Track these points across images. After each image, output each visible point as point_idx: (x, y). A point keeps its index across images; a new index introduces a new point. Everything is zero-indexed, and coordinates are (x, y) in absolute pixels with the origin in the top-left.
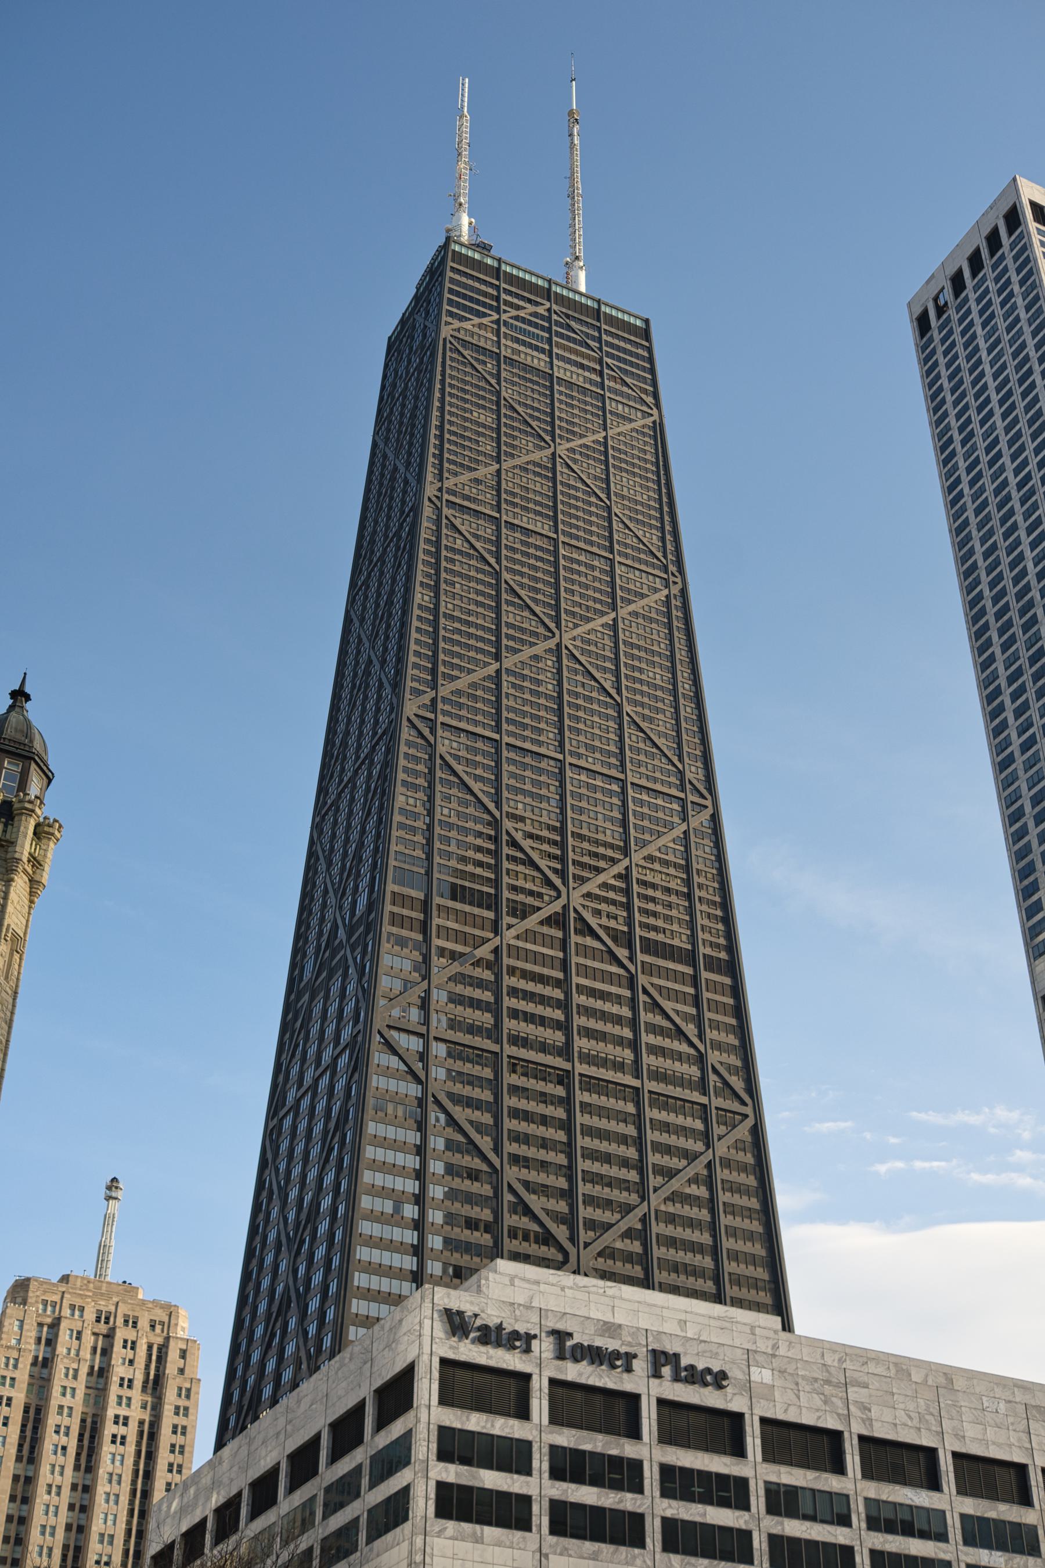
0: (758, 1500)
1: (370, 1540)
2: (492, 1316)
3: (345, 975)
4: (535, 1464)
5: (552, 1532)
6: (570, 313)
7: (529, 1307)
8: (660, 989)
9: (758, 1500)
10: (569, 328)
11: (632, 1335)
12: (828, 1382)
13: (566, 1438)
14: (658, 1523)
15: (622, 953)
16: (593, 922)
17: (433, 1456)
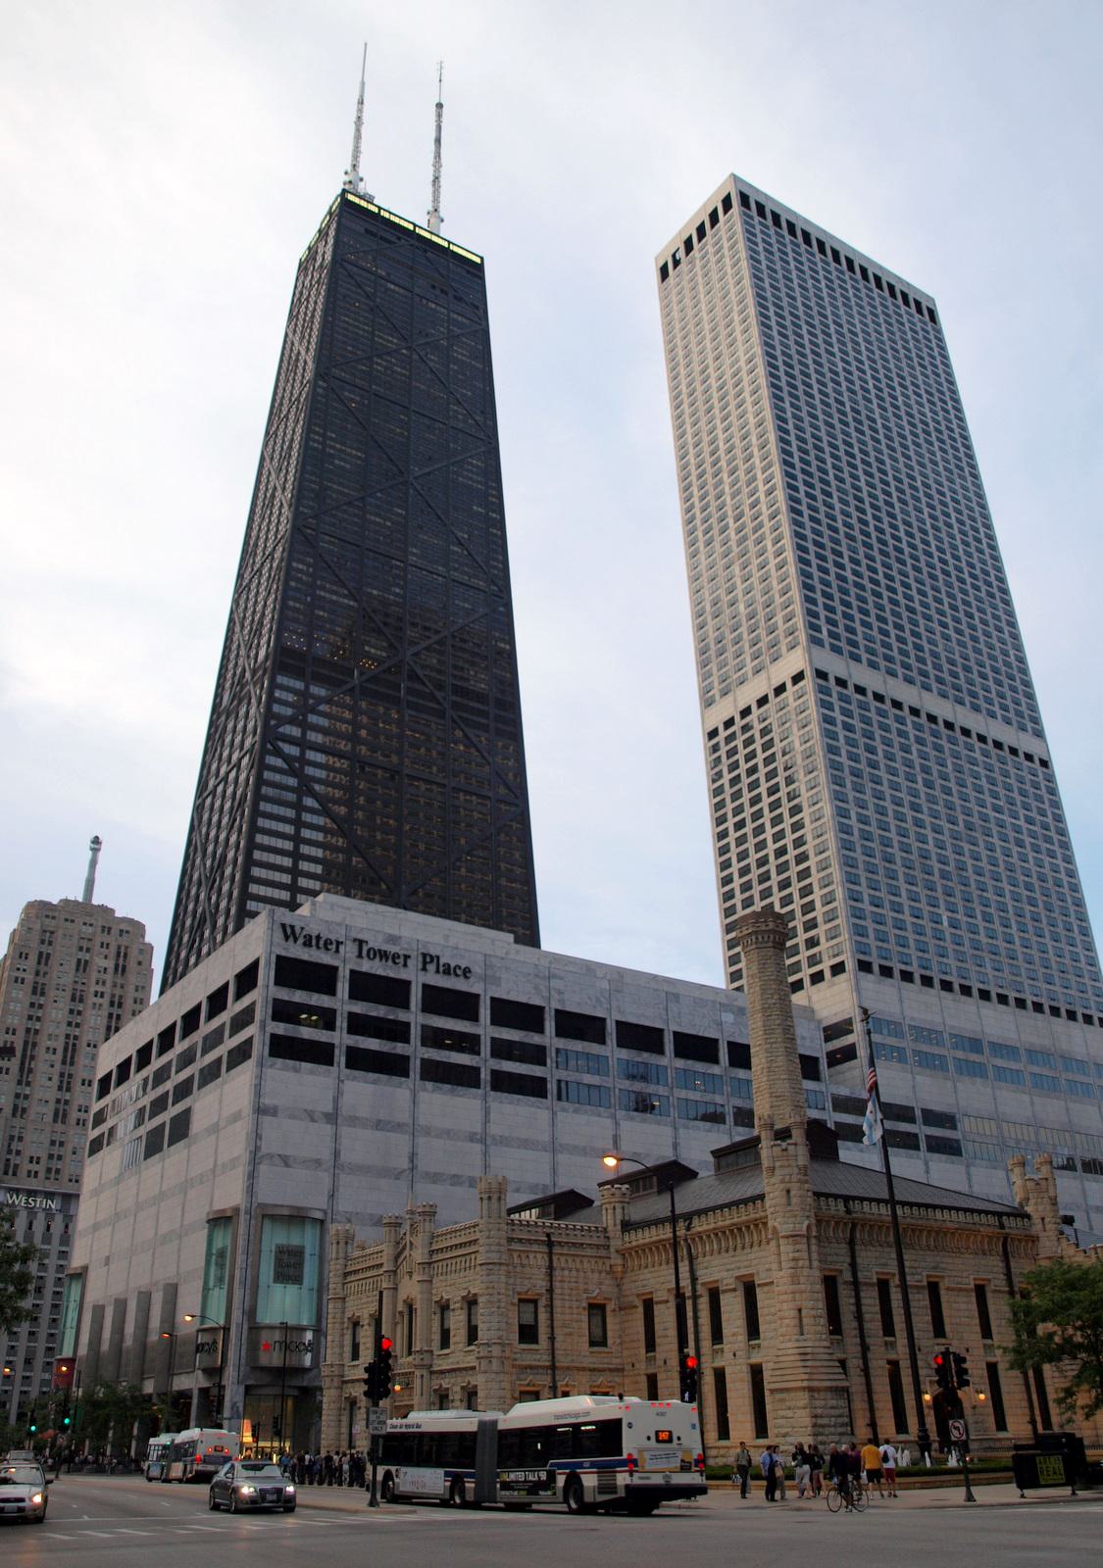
0: (486, 1048)
1: (228, 1070)
2: (314, 929)
3: (249, 703)
4: (338, 1023)
5: (347, 1067)
7: (339, 924)
9: (486, 1048)
11: (409, 943)
12: (537, 976)
13: (359, 1008)
14: (418, 1062)
15: (439, 695)
17: (269, 1018)
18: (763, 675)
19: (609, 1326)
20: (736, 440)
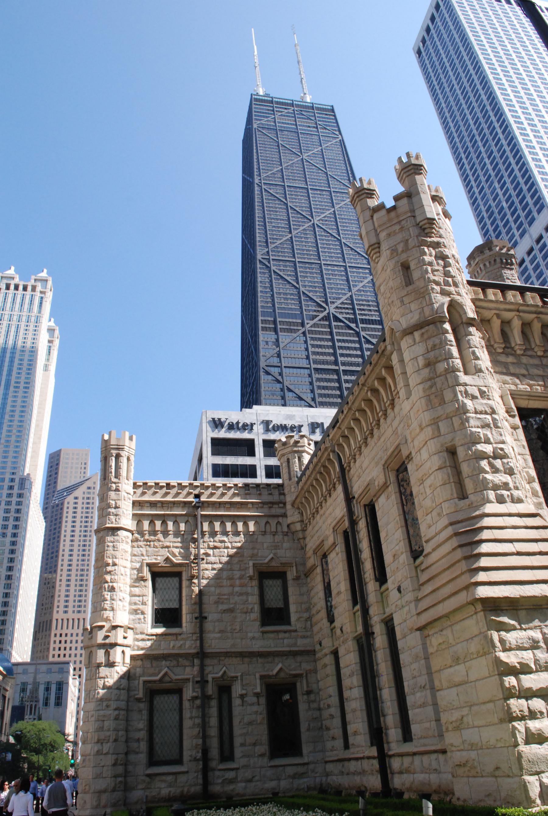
4: (258, 473)
8: (369, 335)
15: (353, 325)
16: (340, 316)
18: (527, 236)
19: (291, 599)
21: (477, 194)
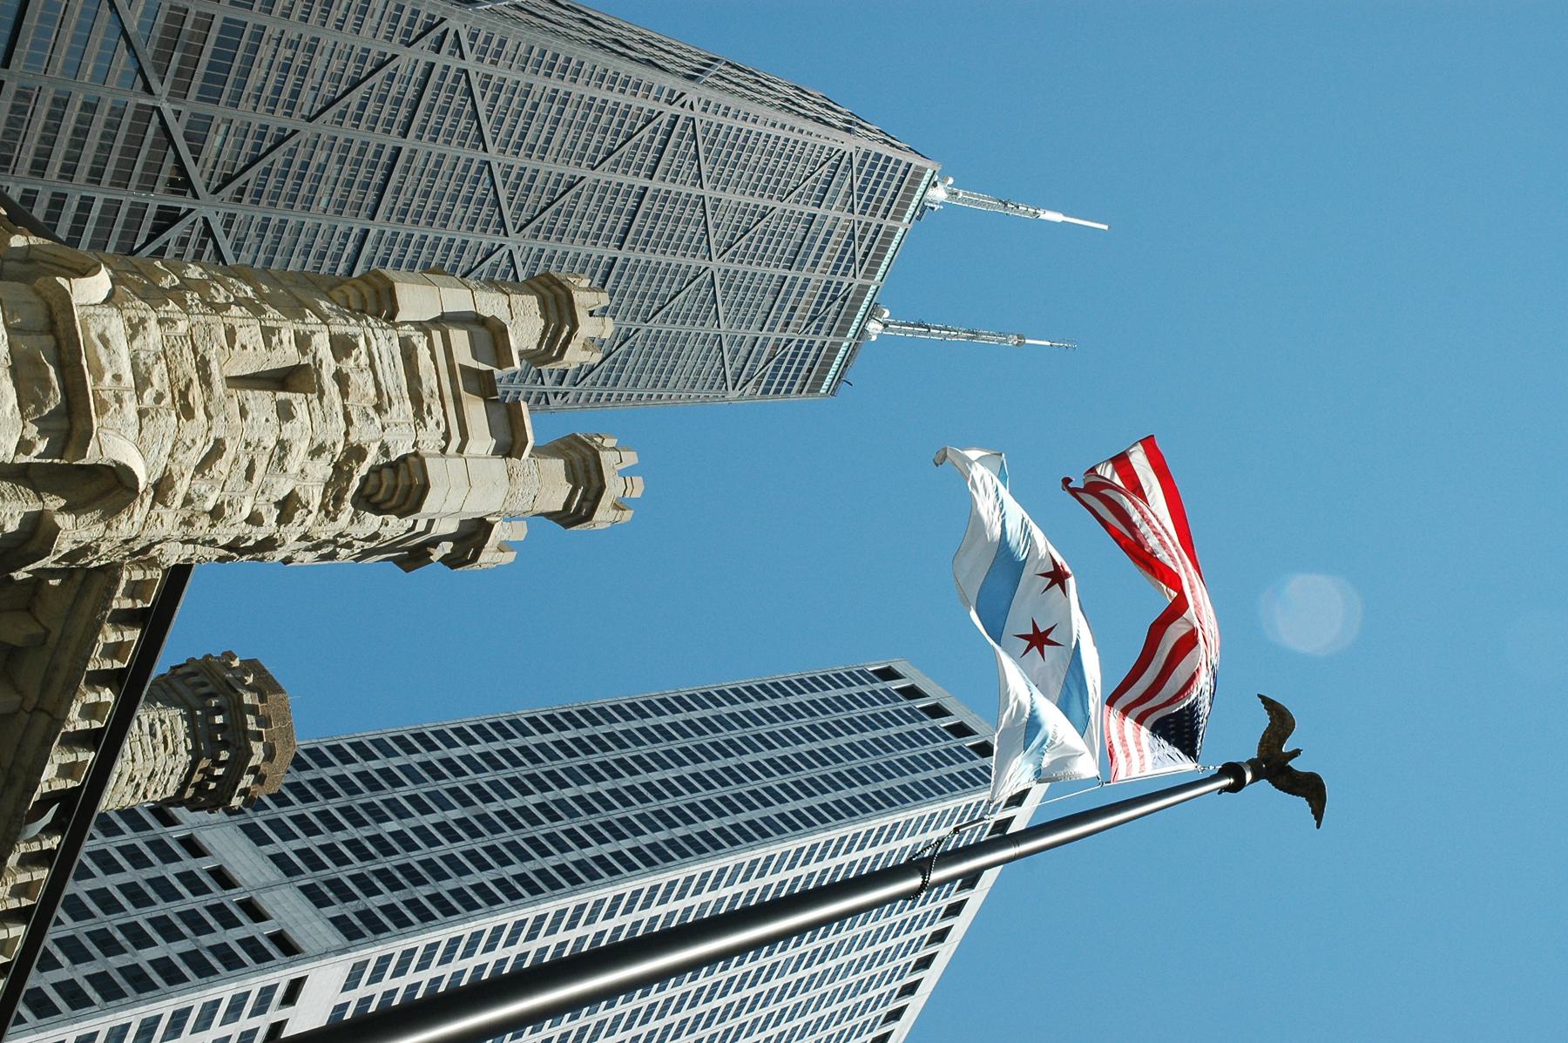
6: (847, 303)
10: (834, 298)
16: (173, 234)
20: (671, 801)
21: (445, 752)
